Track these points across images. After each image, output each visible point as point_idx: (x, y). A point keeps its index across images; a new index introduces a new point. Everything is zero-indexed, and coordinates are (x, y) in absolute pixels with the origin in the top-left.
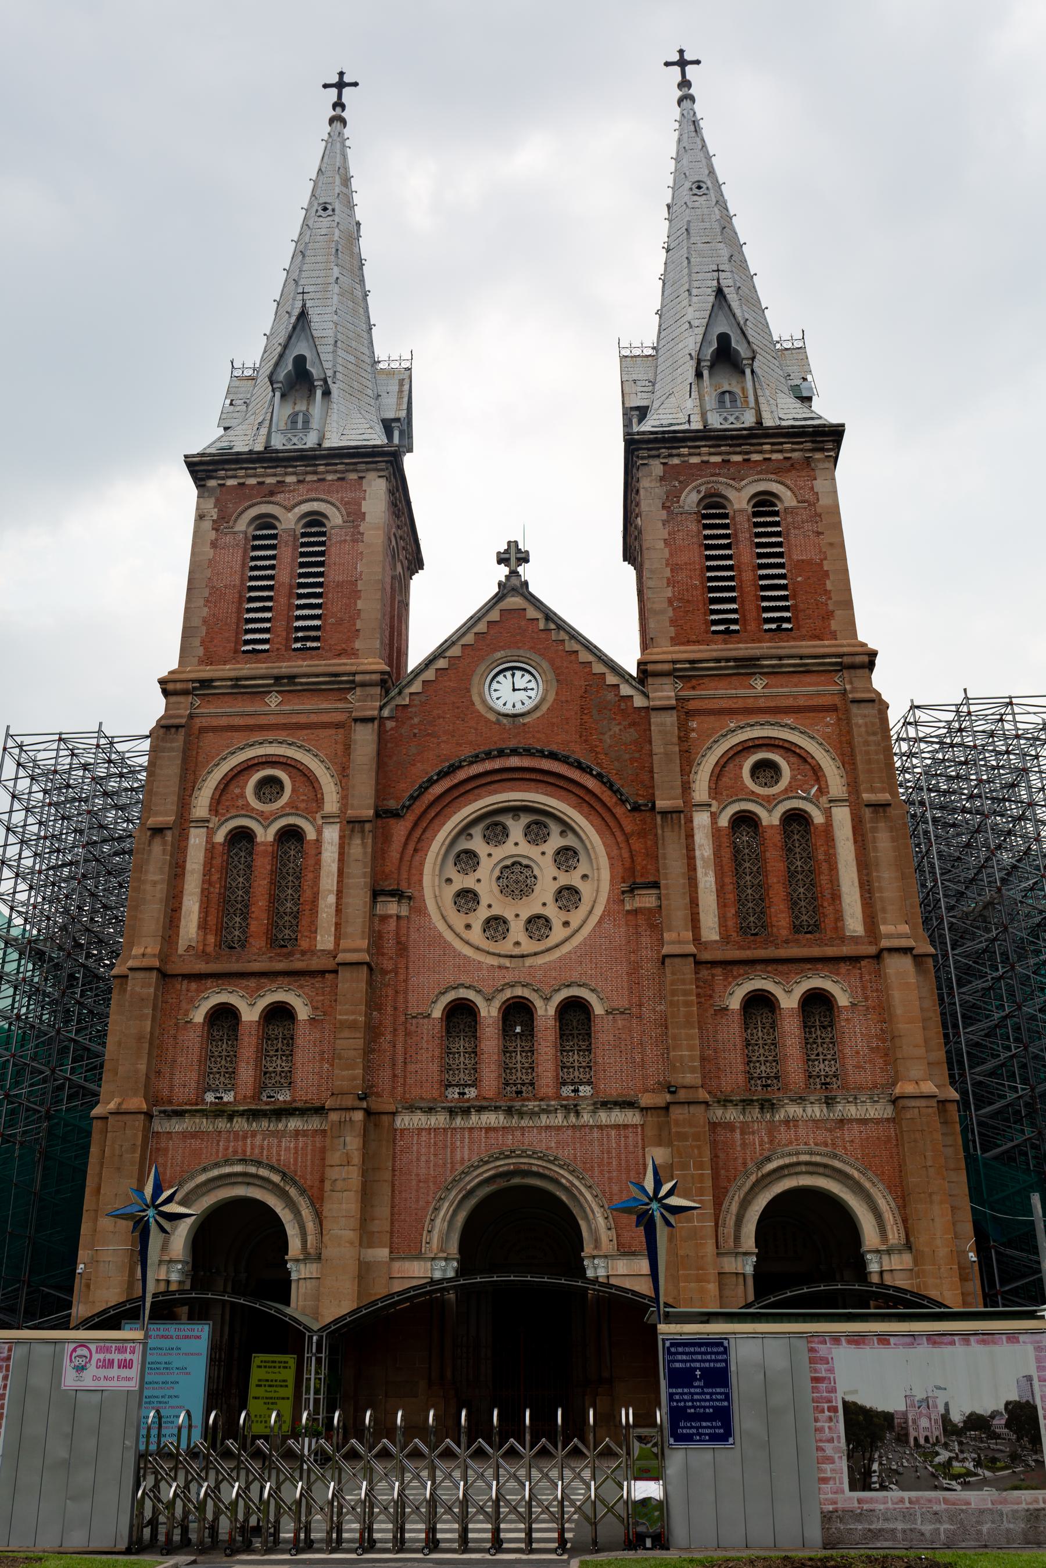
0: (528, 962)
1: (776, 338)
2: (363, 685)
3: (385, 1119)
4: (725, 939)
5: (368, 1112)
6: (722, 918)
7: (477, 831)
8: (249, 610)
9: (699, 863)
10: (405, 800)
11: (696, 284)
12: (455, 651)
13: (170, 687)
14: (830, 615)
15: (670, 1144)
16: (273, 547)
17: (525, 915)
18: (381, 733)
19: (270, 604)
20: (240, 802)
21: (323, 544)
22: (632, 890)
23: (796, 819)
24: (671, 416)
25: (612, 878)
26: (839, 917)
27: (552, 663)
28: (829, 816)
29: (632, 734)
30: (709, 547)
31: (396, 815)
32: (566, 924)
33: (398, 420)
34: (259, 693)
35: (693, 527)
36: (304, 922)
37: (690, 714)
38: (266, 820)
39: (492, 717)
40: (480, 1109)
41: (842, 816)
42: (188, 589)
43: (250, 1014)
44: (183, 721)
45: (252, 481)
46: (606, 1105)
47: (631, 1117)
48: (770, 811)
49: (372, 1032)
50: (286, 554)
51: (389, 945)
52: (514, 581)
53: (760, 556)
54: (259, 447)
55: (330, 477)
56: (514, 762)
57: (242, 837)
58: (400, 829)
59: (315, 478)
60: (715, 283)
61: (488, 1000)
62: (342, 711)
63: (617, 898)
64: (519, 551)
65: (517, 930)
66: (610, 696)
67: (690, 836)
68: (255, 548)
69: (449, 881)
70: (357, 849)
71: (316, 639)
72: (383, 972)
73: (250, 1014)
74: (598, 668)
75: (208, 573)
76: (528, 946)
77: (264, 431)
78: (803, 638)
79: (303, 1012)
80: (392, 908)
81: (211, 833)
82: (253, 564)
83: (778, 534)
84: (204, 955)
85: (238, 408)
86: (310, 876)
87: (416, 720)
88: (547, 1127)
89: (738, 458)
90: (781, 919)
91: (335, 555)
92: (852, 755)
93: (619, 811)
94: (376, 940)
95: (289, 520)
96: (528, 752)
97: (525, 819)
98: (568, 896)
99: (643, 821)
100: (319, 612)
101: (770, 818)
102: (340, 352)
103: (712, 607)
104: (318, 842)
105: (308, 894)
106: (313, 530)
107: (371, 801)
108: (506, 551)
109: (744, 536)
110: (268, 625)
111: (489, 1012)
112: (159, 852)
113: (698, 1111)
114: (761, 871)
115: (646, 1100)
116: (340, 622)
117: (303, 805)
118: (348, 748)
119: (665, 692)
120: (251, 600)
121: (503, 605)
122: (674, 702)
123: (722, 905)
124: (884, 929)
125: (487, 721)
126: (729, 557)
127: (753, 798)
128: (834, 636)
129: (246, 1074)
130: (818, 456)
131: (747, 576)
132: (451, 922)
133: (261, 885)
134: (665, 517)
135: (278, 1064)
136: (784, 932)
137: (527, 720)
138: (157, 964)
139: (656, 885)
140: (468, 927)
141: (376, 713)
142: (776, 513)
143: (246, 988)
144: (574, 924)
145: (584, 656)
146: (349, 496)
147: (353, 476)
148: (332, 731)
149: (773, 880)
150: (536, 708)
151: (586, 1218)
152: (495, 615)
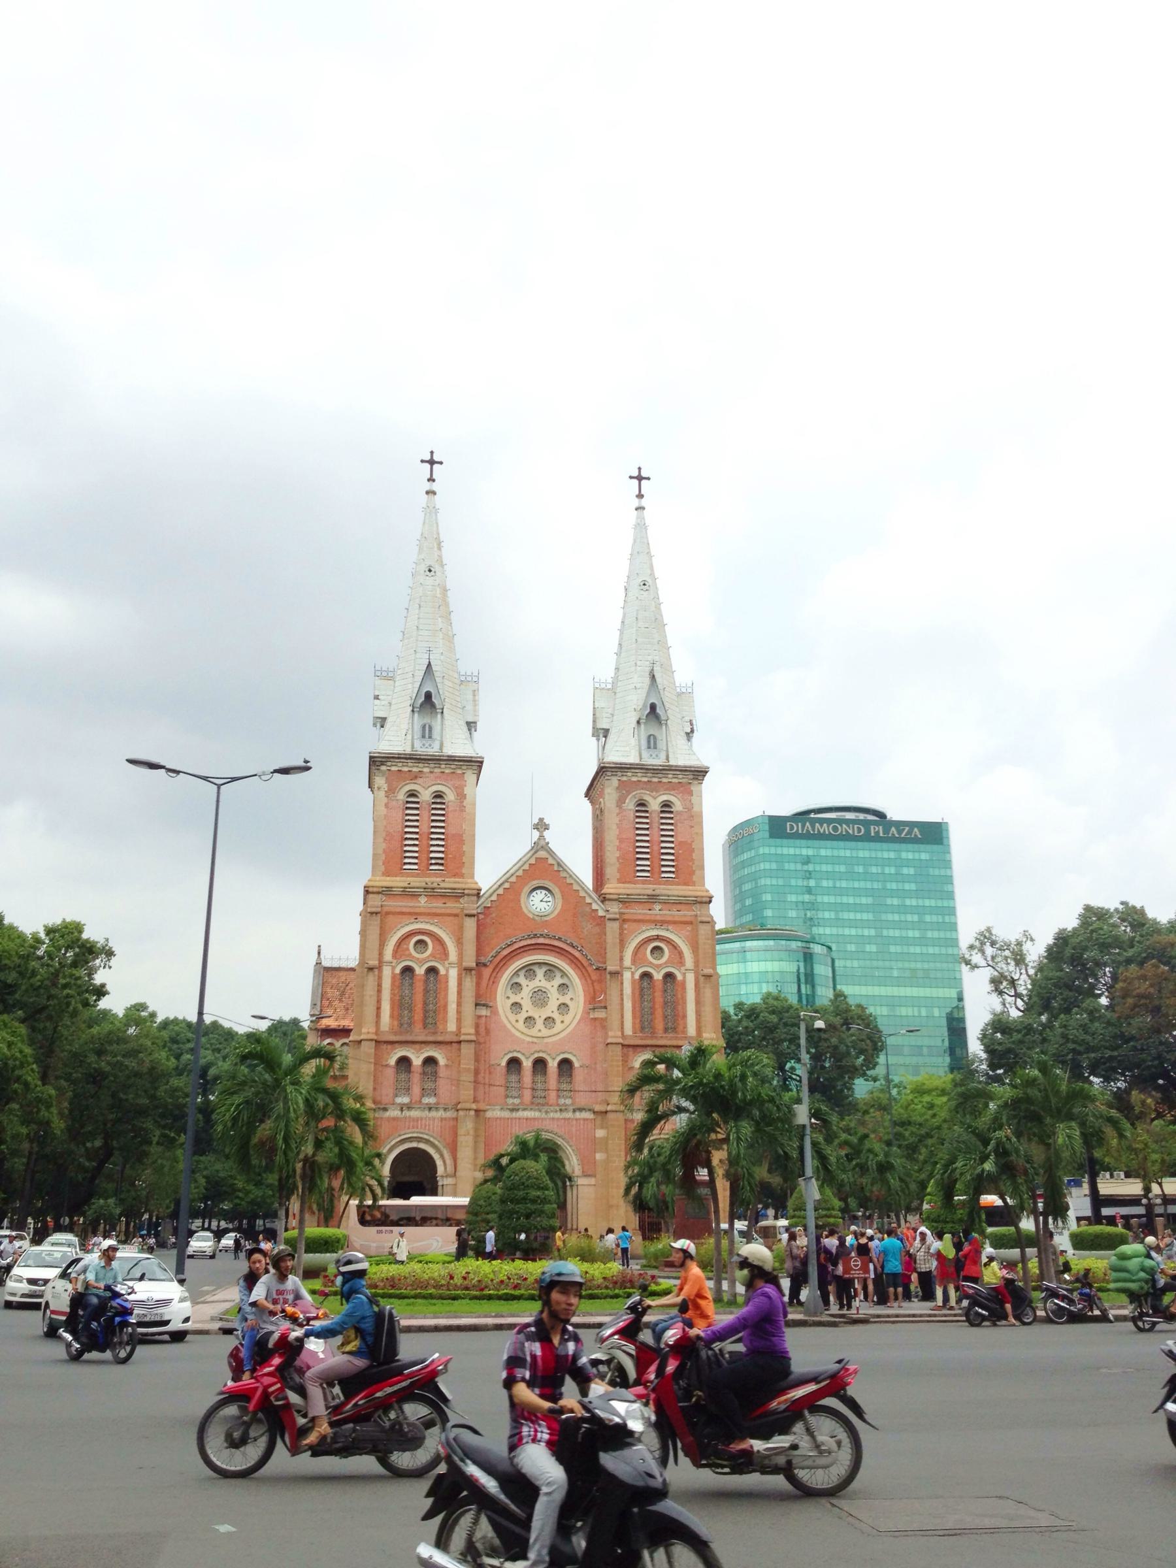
0: (546, 1040)
1: (677, 685)
2: (468, 895)
3: (482, 1113)
4: (634, 1033)
5: (477, 1111)
6: (634, 1023)
7: (522, 973)
8: (406, 845)
9: (625, 997)
10: (489, 958)
11: (640, 658)
12: (513, 879)
13: (371, 890)
14: (692, 873)
15: (607, 1128)
16: (417, 809)
17: (544, 1017)
18: (478, 920)
19: (417, 842)
20: (407, 953)
21: (444, 809)
22: (594, 1009)
23: (669, 976)
24: (623, 749)
25: (585, 1001)
26: (685, 1027)
27: (559, 888)
28: (684, 977)
29: (597, 929)
30: (638, 829)
31: (485, 965)
32: (562, 1022)
33: (475, 723)
34: (415, 896)
35: (632, 815)
36: (441, 1016)
37: (624, 921)
38: (421, 962)
39: (531, 916)
40: (524, 1110)
41: (690, 979)
42: (374, 832)
43: (417, 1061)
44: (379, 910)
45: (406, 769)
46: (581, 1110)
47: (588, 1115)
48: (658, 972)
49: (477, 1072)
50: (425, 815)
51: (482, 1030)
52: (542, 843)
53: (663, 836)
54: (408, 750)
55: (447, 771)
56: (541, 940)
57: (408, 970)
58: (486, 972)
59: (439, 770)
60: (648, 669)
61: (527, 1058)
62: (458, 908)
63: (586, 1013)
64: (546, 825)
65: (540, 1023)
66: (588, 909)
67: (622, 983)
68: (407, 808)
69: (508, 998)
70: (469, 983)
71: (442, 864)
72: (480, 1043)
73: (417, 1061)
74: (582, 894)
75: (385, 823)
76: (545, 1032)
77: (409, 737)
78: (678, 884)
79: (442, 1061)
80: (483, 1012)
81: (393, 968)
82: (407, 818)
83: (672, 824)
84: (395, 1034)
85: (383, 703)
86: (443, 993)
87: (494, 915)
88: (553, 1119)
89: (655, 780)
90: (659, 1025)
91: (451, 818)
92: (697, 948)
93: (588, 969)
94: (477, 1026)
95: (426, 795)
96: (547, 936)
97: (544, 969)
98: (563, 1007)
99: (601, 975)
100: (442, 849)
101: (658, 976)
102: (446, 682)
103: (638, 863)
104: (446, 976)
105: (442, 1002)
106: (438, 800)
107: (474, 959)
108: (538, 824)
109: (655, 825)
110: (416, 855)
111: (527, 1064)
112: (371, 980)
113: (620, 1115)
114: (653, 1001)
115: (597, 1108)
116: (454, 858)
117: (438, 956)
118: (461, 928)
119: (614, 908)
120: (406, 839)
121: (537, 855)
122: (617, 916)
123: (634, 1017)
124: (705, 1035)
125: (529, 918)
126: (647, 835)
127: (651, 965)
128: (694, 884)
129: (416, 1090)
130: (696, 782)
131: (656, 848)
132: (510, 1019)
133: (419, 998)
134: (618, 811)
135: (429, 1085)
136: (661, 1032)
137: (546, 919)
138: (375, 1037)
139: (605, 1008)
140: (517, 1021)
141: (475, 912)
142: (671, 812)
143: (415, 1049)
144: (567, 1022)
145: (575, 887)
146: (458, 783)
147: (459, 771)
148: (452, 918)
149: (657, 1006)
150: (552, 912)
151: (569, 1159)
152: (533, 861)
